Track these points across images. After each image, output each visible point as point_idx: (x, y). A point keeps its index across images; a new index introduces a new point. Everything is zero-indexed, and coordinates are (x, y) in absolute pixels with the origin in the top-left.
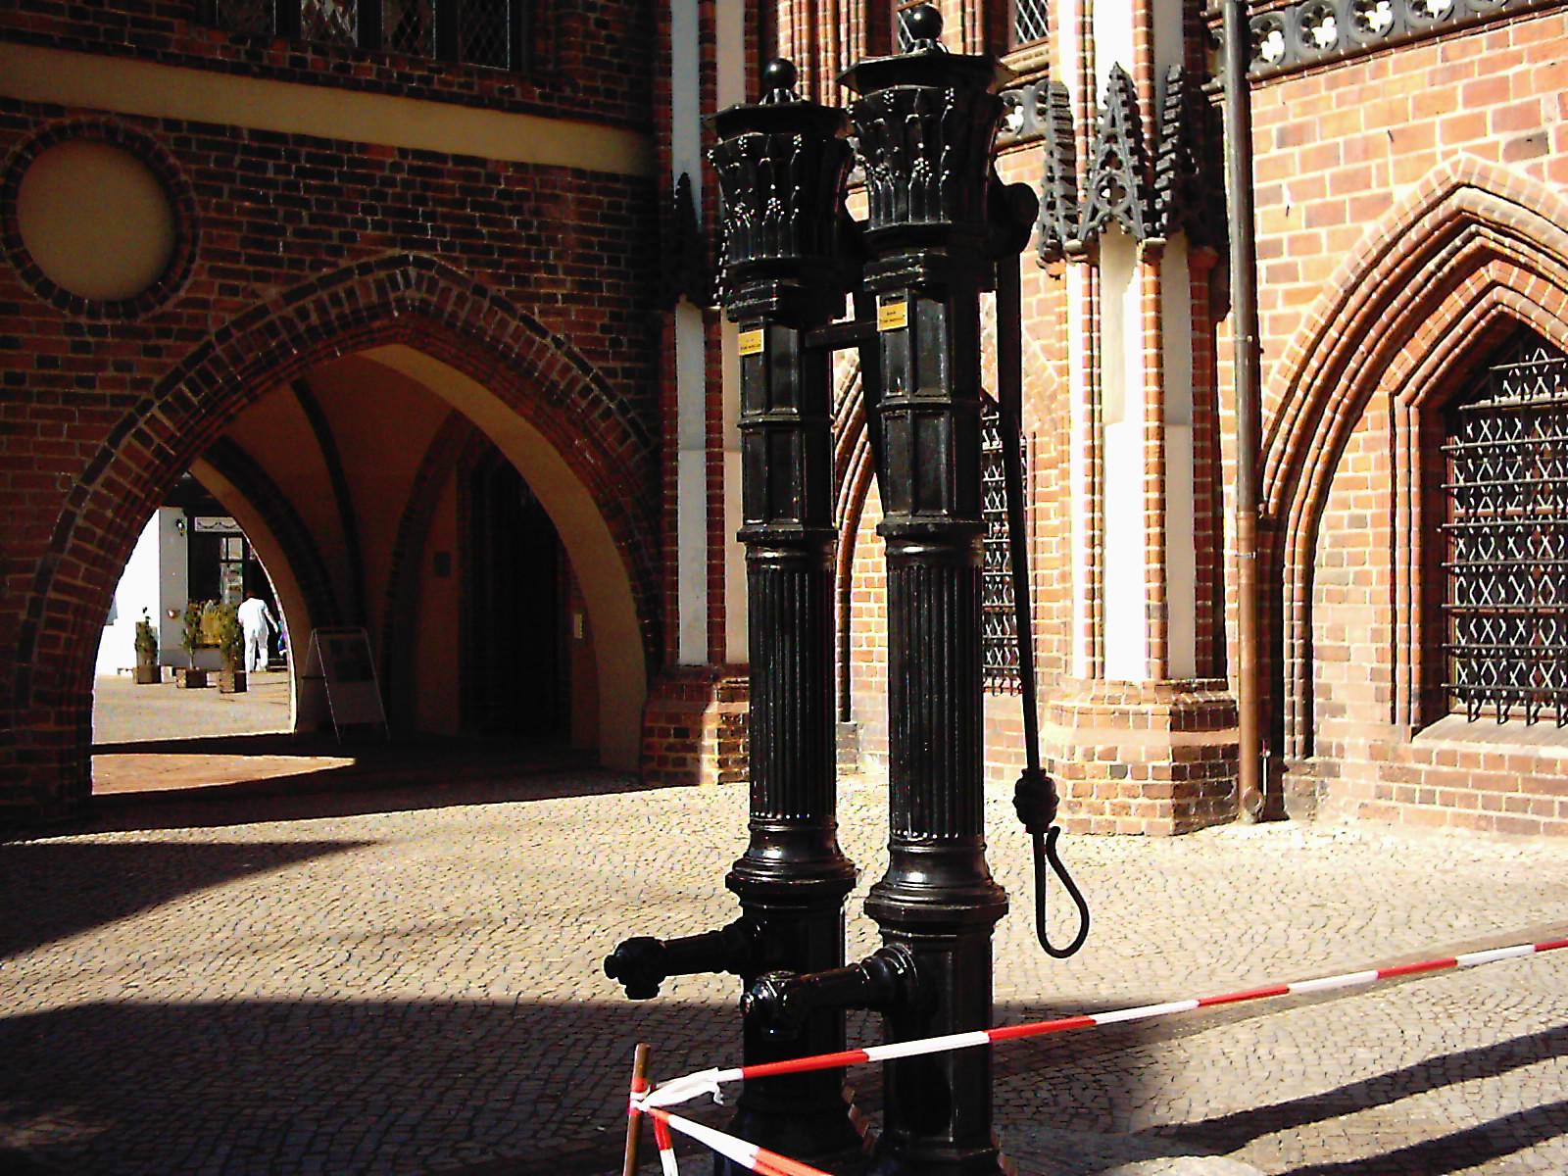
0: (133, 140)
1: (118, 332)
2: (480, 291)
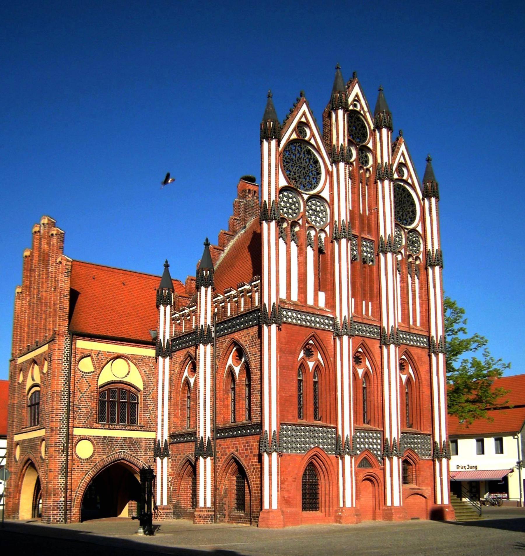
1: (87, 462)
2: (131, 455)
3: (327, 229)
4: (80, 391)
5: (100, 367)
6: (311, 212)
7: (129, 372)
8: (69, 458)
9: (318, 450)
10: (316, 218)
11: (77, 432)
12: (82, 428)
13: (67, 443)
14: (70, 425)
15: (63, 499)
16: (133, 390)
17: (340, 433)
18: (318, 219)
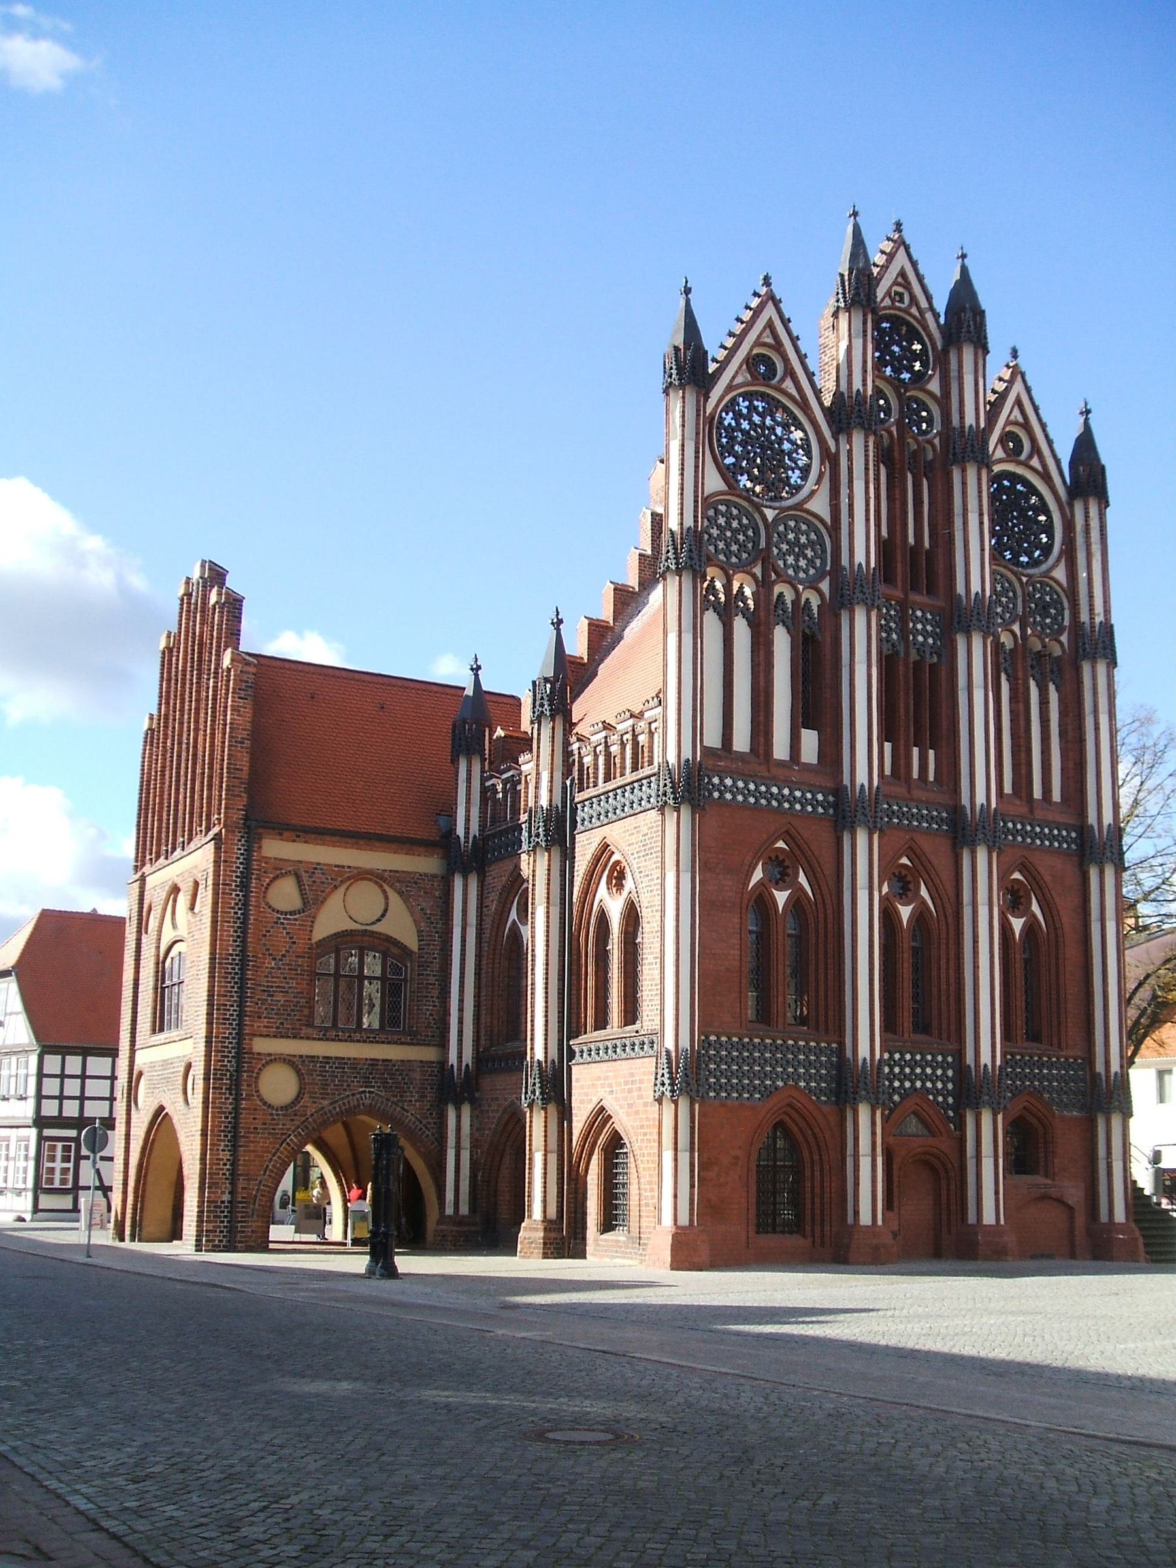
0: (289, 1061)
2: (388, 1100)
3: (825, 586)
4: (270, 955)
5: (312, 901)
6: (785, 547)
7: (386, 910)
8: (244, 1104)
9: (796, 1094)
10: (797, 560)
11: (262, 1045)
12: (275, 1036)
13: (238, 1070)
14: (247, 1030)
15: (226, 1197)
16: (395, 950)
17: (849, 1054)
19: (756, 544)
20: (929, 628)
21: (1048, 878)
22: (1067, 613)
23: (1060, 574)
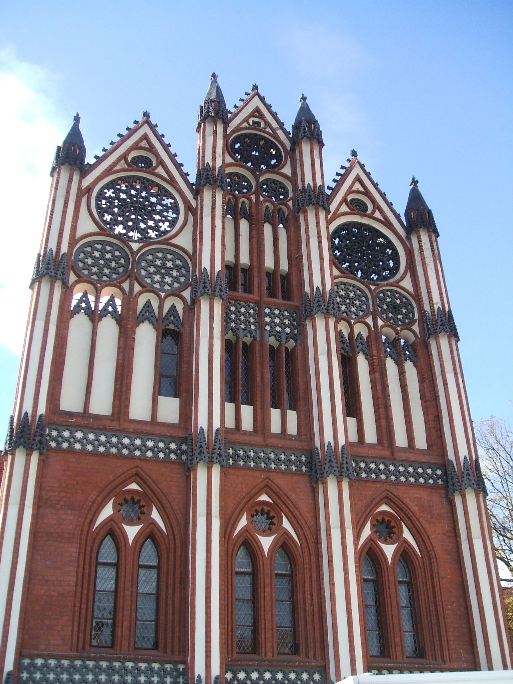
18: (152, 269)
19: (125, 267)
20: (287, 322)
21: (415, 508)
22: (416, 311)
23: (407, 283)
